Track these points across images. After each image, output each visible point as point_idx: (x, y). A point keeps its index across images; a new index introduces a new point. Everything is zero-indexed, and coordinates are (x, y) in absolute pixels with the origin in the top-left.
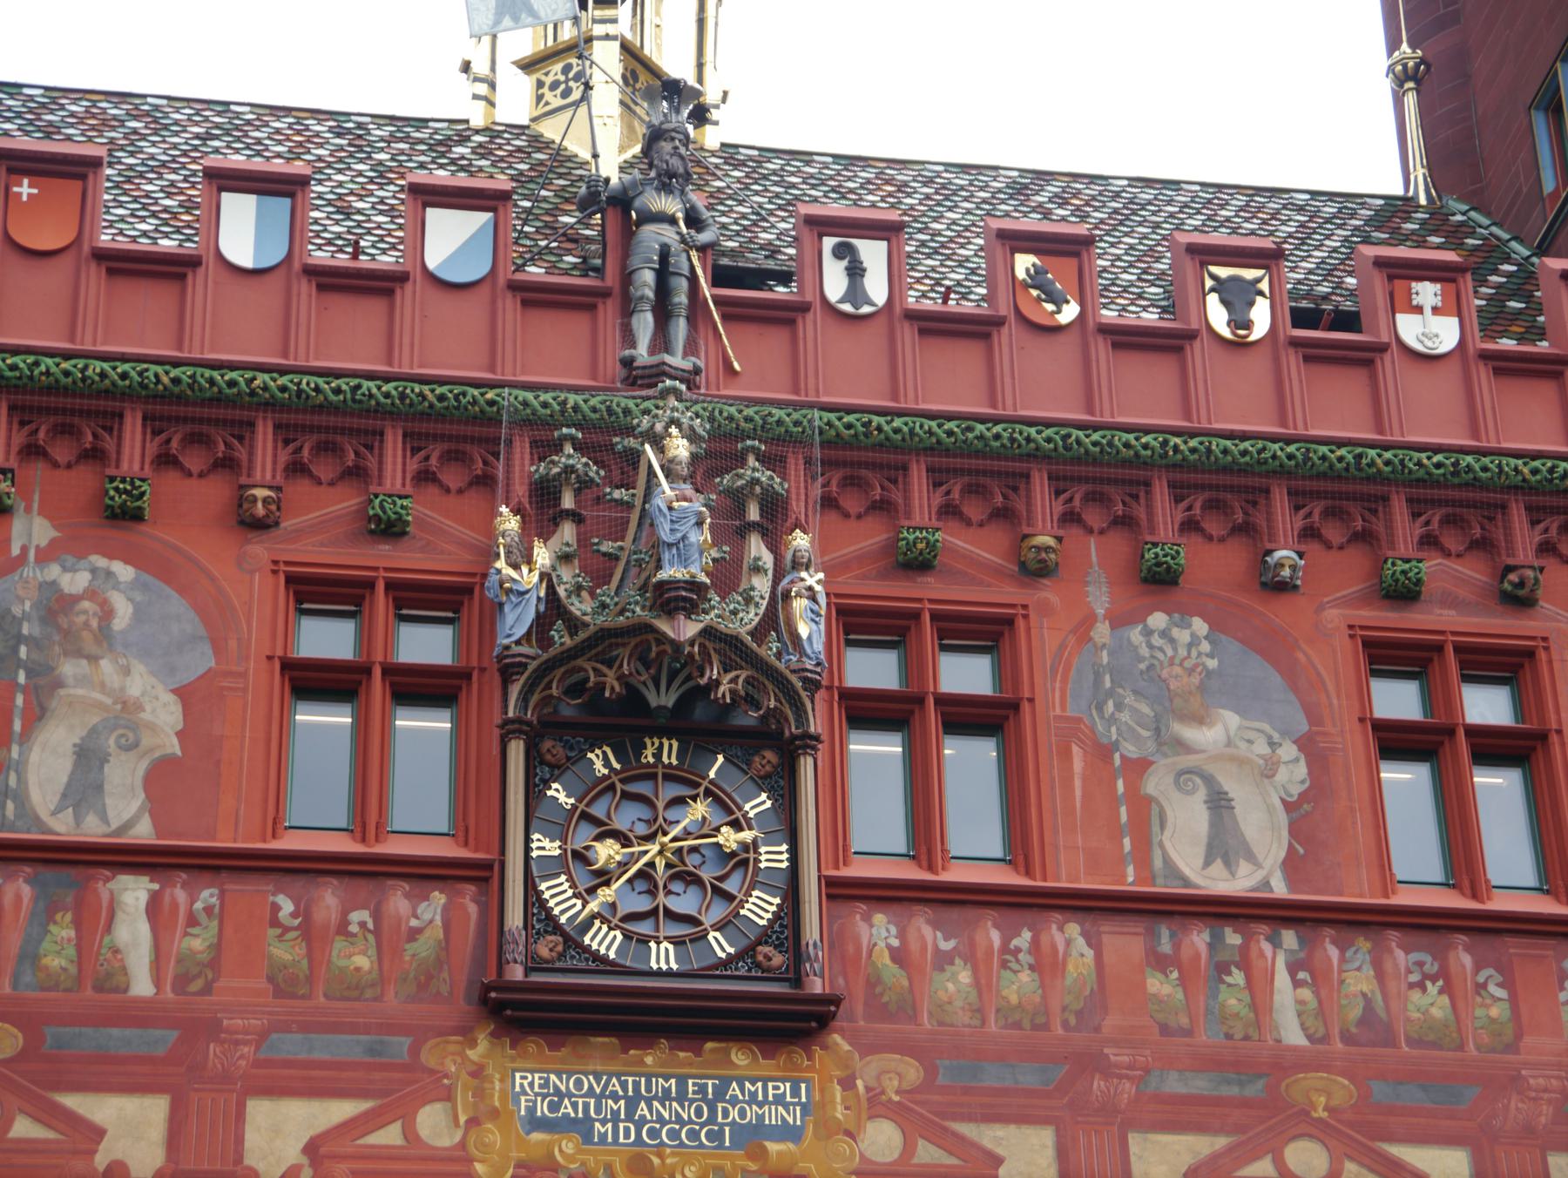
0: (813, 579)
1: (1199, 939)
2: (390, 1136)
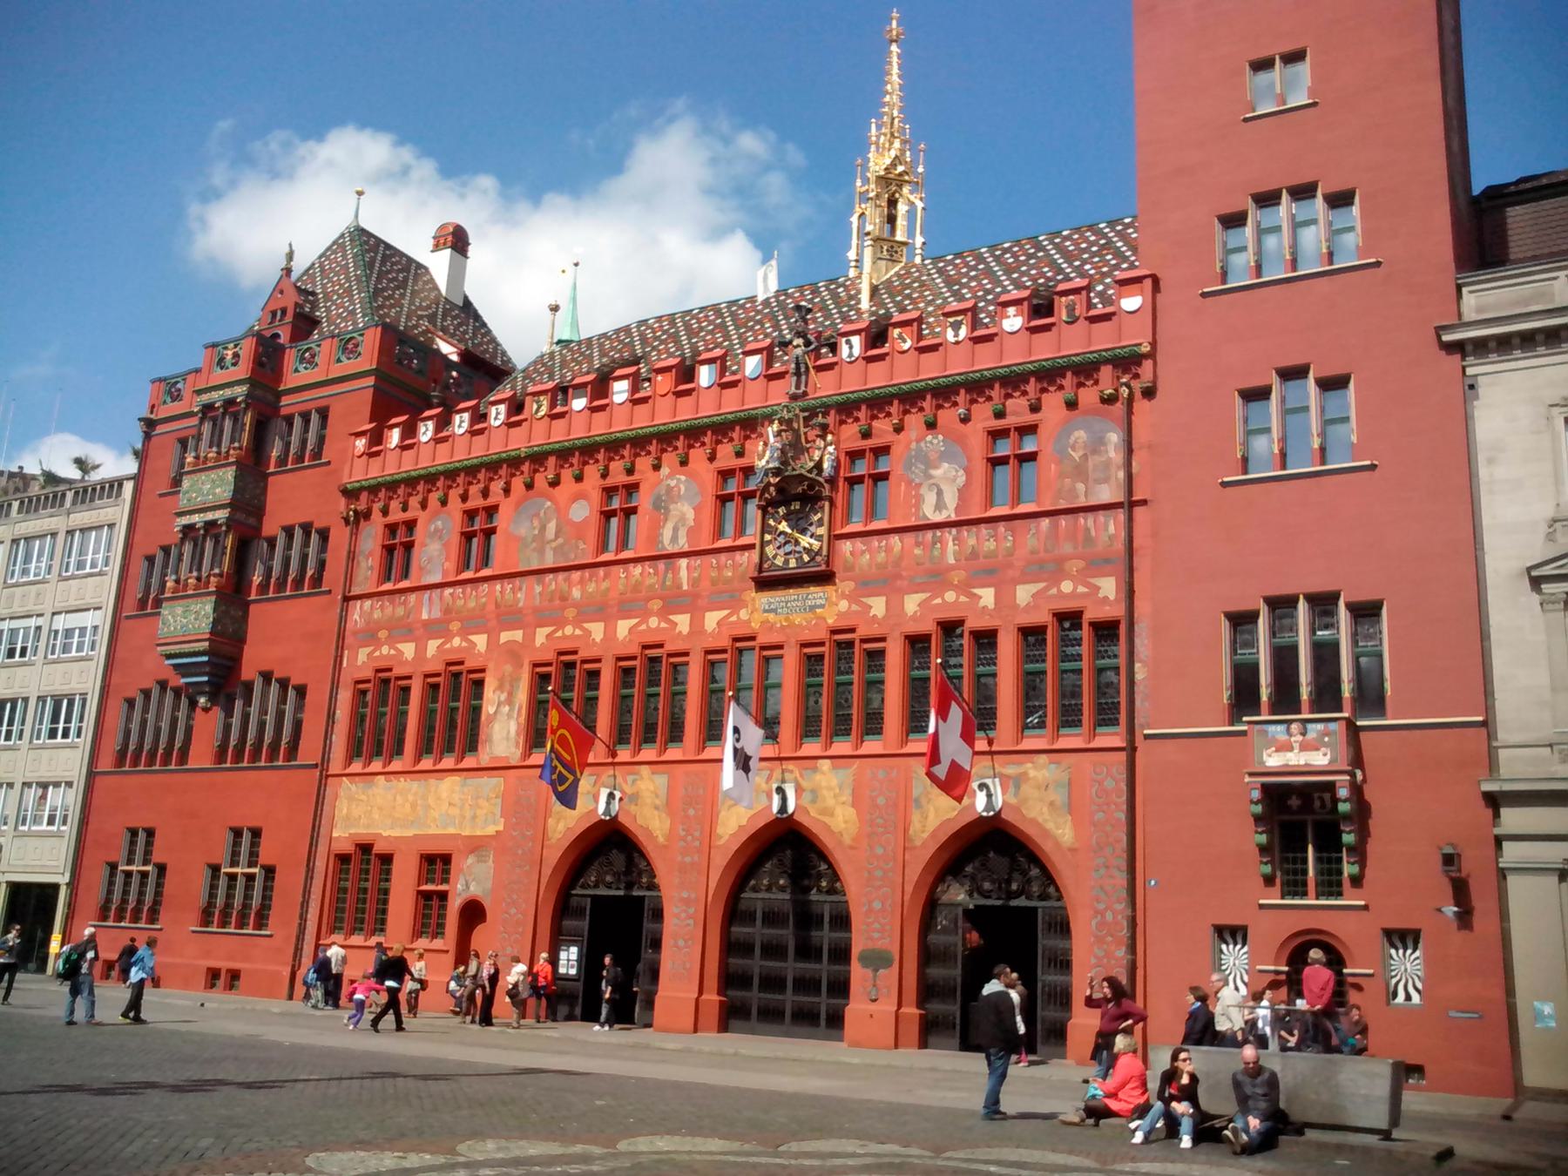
0: (831, 449)
1: (929, 535)
2: (734, 618)
